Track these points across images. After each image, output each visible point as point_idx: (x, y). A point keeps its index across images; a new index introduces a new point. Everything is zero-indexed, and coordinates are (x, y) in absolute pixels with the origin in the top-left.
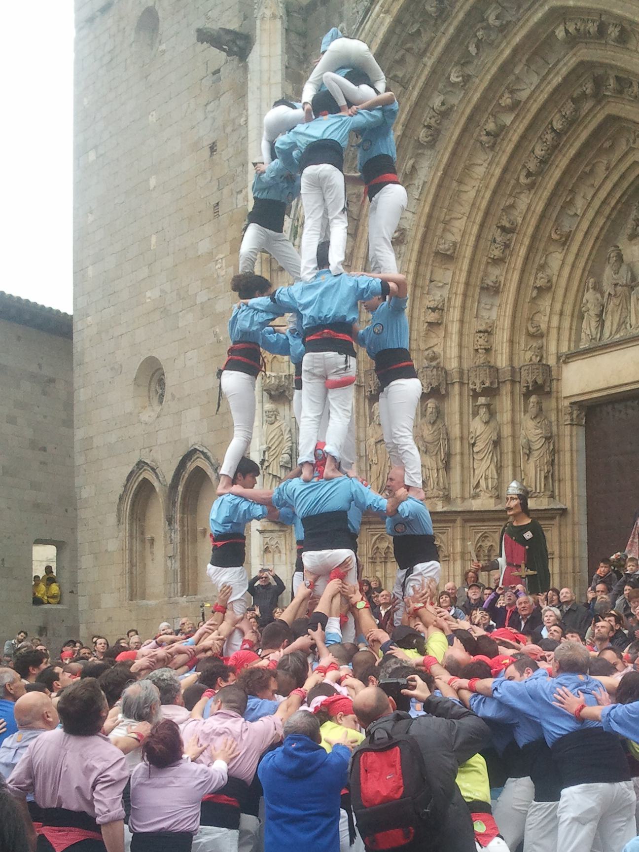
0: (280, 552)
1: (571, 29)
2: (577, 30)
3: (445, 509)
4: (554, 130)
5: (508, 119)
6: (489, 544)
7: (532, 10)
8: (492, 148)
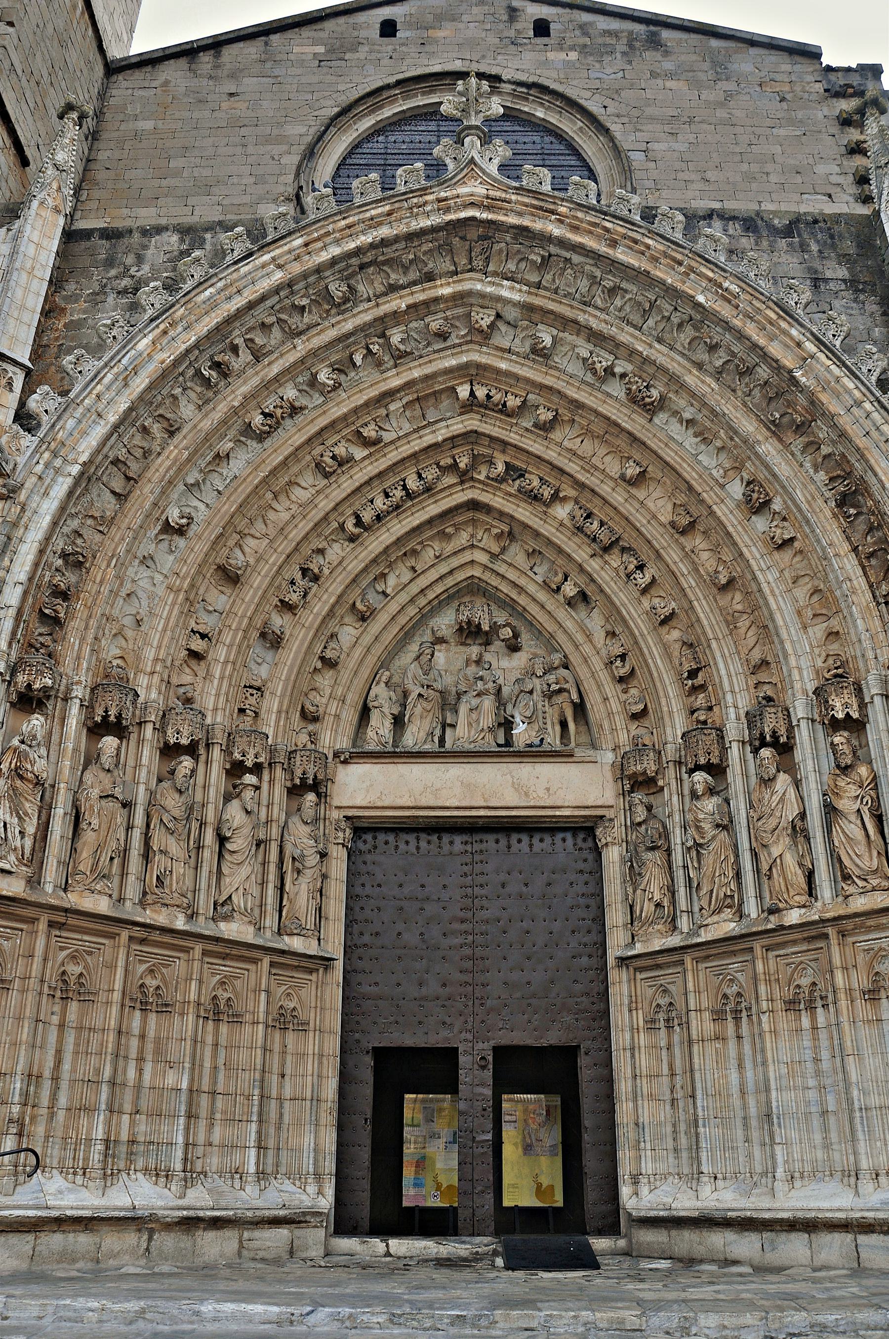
1: (481, 393)
2: (489, 397)
3: (187, 928)
4: (404, 487)
5: (359, 453)
6: (226, 995)
7: (442, 354)
8: (327, 475)
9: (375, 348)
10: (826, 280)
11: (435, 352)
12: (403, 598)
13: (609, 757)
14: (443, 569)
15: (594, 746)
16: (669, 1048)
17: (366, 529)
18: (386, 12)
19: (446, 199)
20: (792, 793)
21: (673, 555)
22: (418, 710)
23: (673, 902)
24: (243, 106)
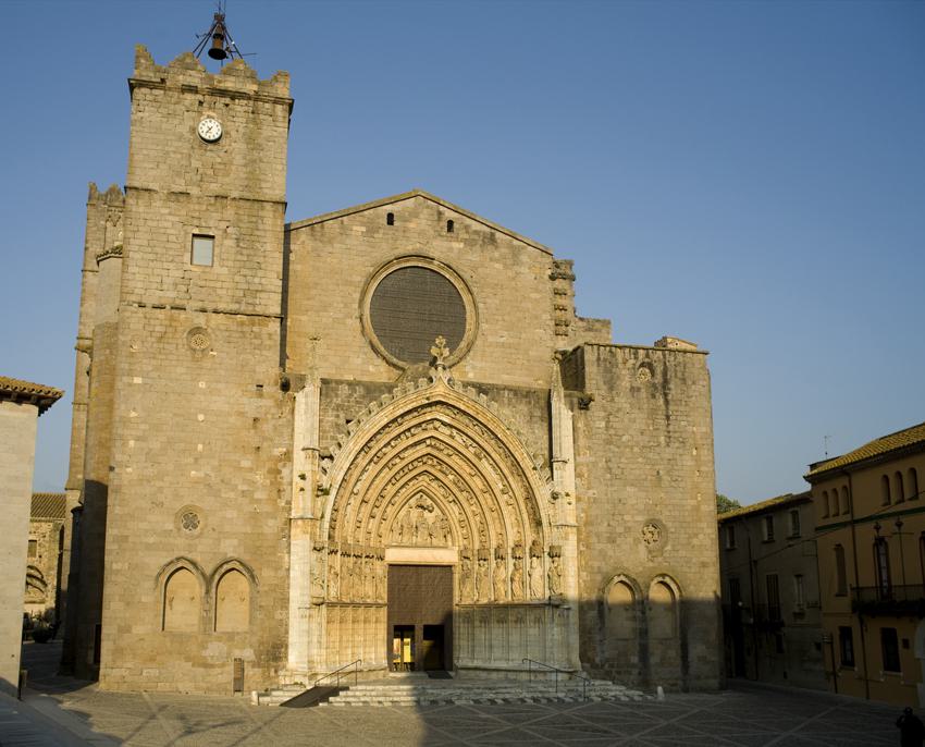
18: (389, 208)
21: (481, 498)
24: (335, 261)
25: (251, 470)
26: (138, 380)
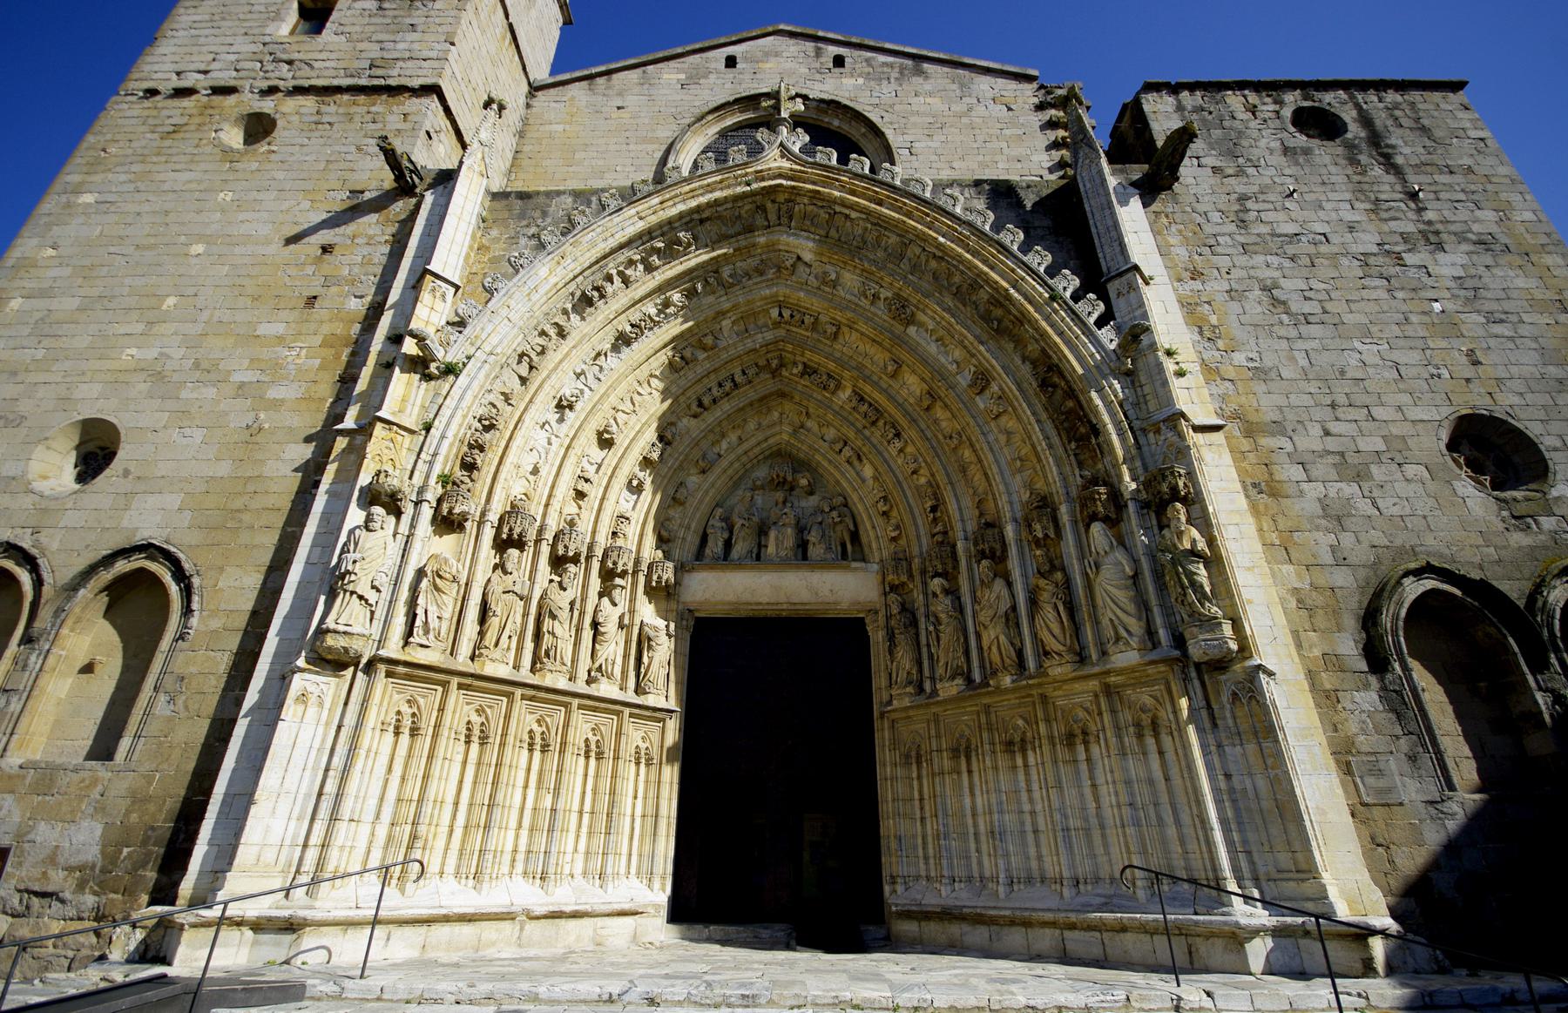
0: (321, 705)
2: (792, 316)
4: (733, 380)
5: (702, 356)
9: (711, 280)
10: (1035, 228)
11: (756, 284)
12: (732, 457)
13: (876, 567)
14: (760, 436)
15: (864, 560)
16: (919, 777)
17: (705, 409)
18: (730, 50)
19: (761, 171)
20: (1005, 592)
22: (743, 533)
23: (920, 671)
25: (280, 339)
26: (88, 198)
